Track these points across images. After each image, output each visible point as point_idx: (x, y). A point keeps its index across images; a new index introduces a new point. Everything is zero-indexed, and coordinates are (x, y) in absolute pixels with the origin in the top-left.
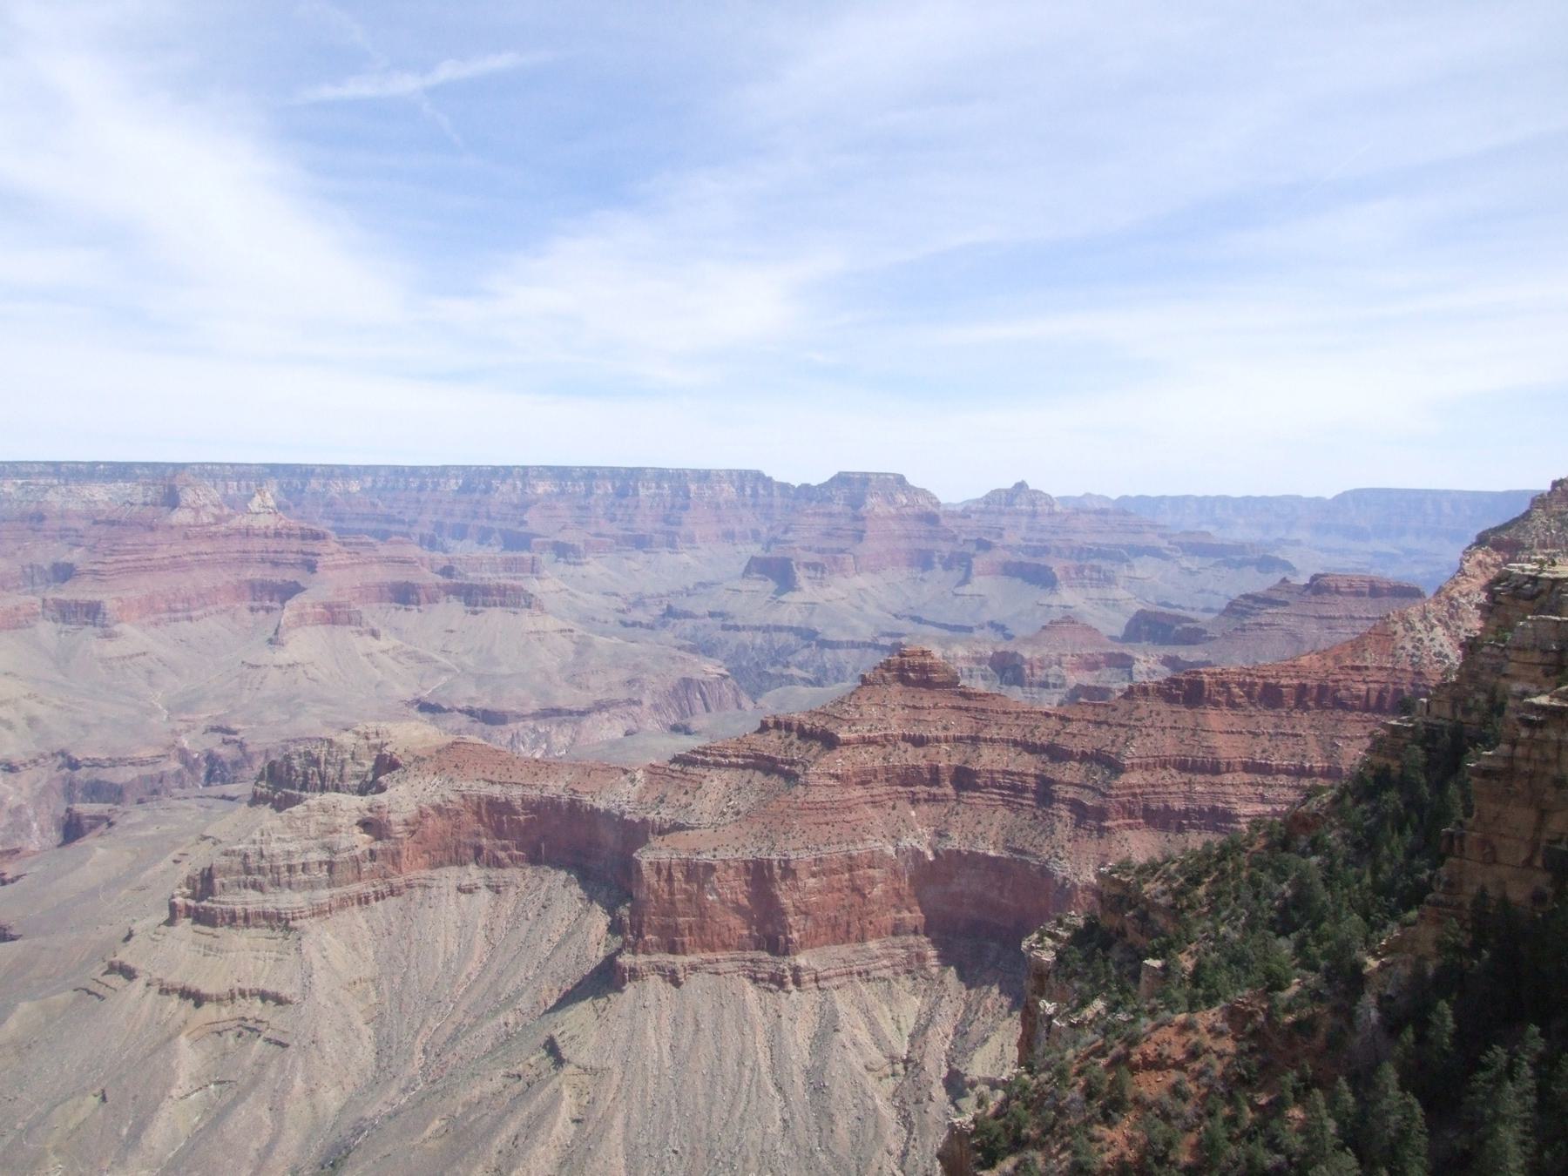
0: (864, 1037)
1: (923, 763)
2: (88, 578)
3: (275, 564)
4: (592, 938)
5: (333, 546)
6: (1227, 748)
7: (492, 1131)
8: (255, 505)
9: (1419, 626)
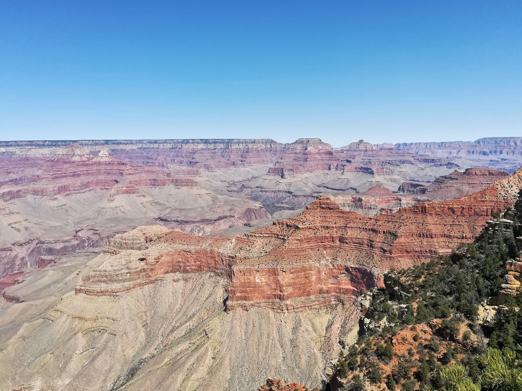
0: (310, 328)
1: (328, 235)
2: (44, 180)
3: (109, 174)
4: (218, 296)
5: (129, 167)
6: (434, 229)
7: (185, 363)
8: (100, 154)
9: (507, 186)
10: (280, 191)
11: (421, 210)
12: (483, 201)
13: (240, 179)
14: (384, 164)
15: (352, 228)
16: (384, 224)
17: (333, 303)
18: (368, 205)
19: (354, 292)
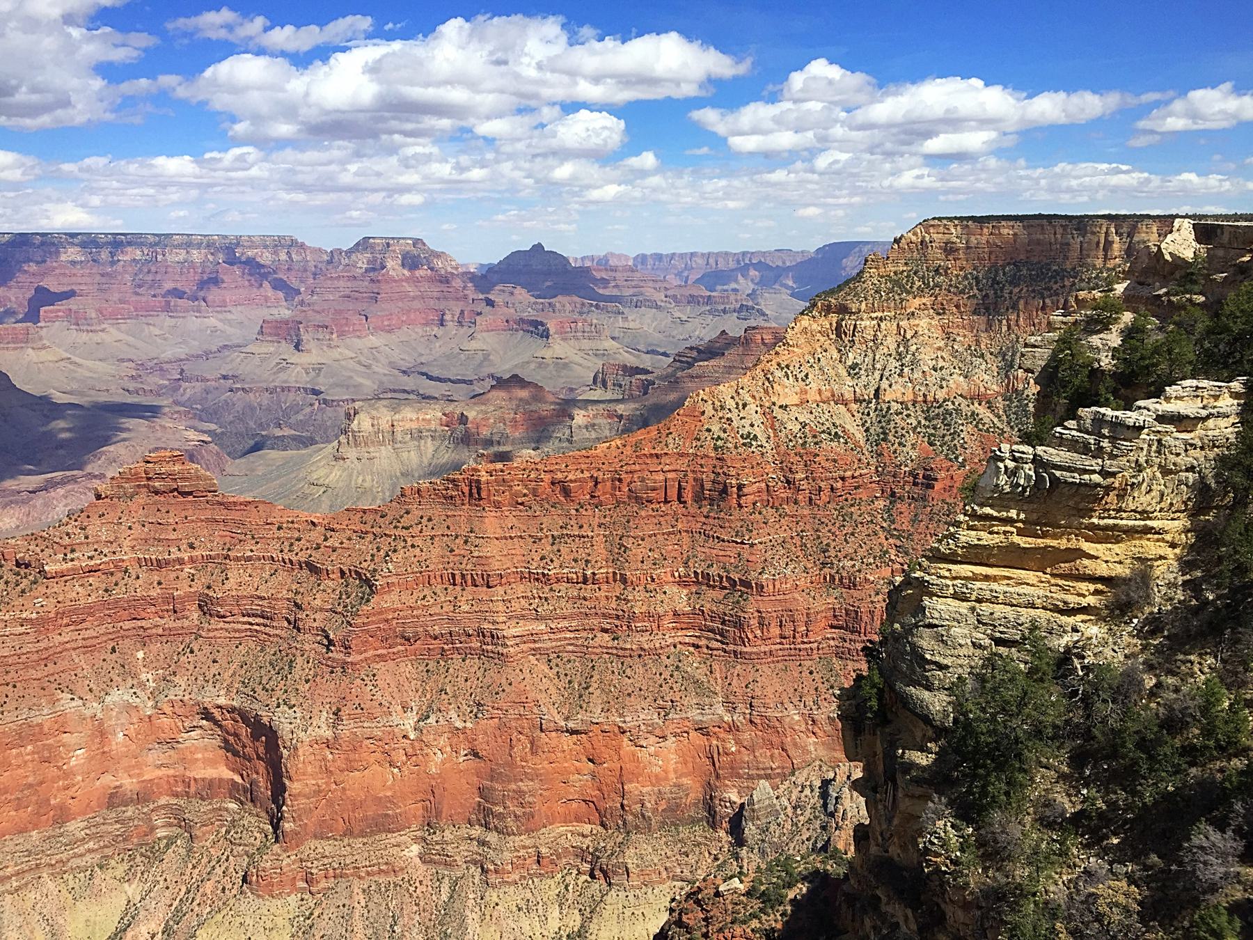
9: (731, 404)
10: (289, 389)
11: (466, 490)
12: (657, 456)
13: (181, 352)
14: (585, 310)
15: (249, 559)
16: (346, 544)
17: (161, 833)
18: (485, 432)
19: (233, 791)
